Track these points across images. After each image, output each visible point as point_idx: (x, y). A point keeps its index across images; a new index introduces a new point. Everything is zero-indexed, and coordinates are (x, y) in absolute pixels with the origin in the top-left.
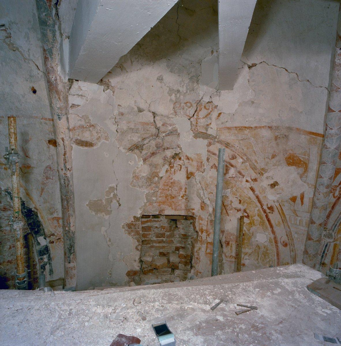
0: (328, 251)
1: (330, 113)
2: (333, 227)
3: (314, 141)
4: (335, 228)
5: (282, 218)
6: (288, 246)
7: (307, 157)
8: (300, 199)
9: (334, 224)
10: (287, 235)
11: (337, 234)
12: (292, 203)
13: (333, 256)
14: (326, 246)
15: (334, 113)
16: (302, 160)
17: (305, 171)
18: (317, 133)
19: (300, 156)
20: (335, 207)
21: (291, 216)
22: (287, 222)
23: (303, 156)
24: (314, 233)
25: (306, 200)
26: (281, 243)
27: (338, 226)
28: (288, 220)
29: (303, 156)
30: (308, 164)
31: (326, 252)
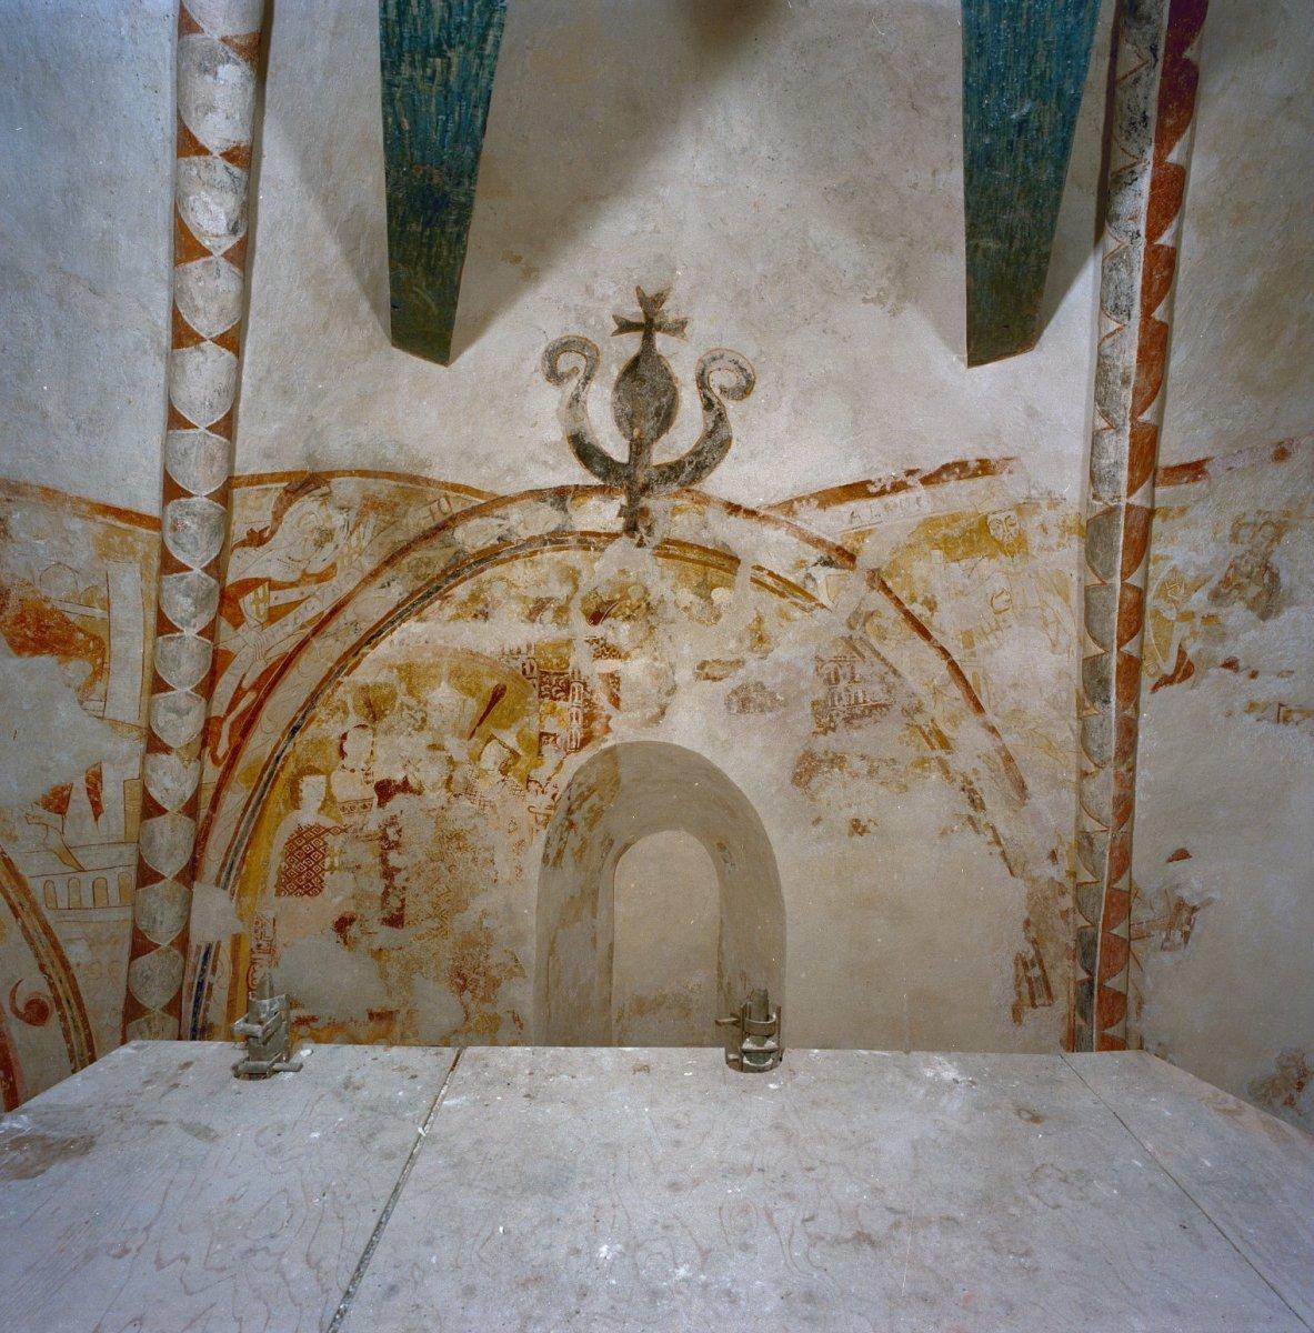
1: (178, 432)
2: (224, 874)
3: (121, 543)
4: (228, 879)
5: (13, 896)
6: (55, 1015)
7: (98, 612)
8: (84, 795)
9: (224, 865)
10: (42, 967)
11: (239, 897)
12: (53, 819)
13: (233, 986)
15: (191, 431)
16: (79, 624)
17: (95, 673)
18: (135, 509)
19: (68, 607)
20: (222, 800)
21: (51, 878)
22: (35, 910)
23: (81, 610)
24: (159, 918)
25: (111, 792)
26: (16, 1012)
28: (39, 899)
29: (81, 610)
30: (107, 643)
31: (209, 978)
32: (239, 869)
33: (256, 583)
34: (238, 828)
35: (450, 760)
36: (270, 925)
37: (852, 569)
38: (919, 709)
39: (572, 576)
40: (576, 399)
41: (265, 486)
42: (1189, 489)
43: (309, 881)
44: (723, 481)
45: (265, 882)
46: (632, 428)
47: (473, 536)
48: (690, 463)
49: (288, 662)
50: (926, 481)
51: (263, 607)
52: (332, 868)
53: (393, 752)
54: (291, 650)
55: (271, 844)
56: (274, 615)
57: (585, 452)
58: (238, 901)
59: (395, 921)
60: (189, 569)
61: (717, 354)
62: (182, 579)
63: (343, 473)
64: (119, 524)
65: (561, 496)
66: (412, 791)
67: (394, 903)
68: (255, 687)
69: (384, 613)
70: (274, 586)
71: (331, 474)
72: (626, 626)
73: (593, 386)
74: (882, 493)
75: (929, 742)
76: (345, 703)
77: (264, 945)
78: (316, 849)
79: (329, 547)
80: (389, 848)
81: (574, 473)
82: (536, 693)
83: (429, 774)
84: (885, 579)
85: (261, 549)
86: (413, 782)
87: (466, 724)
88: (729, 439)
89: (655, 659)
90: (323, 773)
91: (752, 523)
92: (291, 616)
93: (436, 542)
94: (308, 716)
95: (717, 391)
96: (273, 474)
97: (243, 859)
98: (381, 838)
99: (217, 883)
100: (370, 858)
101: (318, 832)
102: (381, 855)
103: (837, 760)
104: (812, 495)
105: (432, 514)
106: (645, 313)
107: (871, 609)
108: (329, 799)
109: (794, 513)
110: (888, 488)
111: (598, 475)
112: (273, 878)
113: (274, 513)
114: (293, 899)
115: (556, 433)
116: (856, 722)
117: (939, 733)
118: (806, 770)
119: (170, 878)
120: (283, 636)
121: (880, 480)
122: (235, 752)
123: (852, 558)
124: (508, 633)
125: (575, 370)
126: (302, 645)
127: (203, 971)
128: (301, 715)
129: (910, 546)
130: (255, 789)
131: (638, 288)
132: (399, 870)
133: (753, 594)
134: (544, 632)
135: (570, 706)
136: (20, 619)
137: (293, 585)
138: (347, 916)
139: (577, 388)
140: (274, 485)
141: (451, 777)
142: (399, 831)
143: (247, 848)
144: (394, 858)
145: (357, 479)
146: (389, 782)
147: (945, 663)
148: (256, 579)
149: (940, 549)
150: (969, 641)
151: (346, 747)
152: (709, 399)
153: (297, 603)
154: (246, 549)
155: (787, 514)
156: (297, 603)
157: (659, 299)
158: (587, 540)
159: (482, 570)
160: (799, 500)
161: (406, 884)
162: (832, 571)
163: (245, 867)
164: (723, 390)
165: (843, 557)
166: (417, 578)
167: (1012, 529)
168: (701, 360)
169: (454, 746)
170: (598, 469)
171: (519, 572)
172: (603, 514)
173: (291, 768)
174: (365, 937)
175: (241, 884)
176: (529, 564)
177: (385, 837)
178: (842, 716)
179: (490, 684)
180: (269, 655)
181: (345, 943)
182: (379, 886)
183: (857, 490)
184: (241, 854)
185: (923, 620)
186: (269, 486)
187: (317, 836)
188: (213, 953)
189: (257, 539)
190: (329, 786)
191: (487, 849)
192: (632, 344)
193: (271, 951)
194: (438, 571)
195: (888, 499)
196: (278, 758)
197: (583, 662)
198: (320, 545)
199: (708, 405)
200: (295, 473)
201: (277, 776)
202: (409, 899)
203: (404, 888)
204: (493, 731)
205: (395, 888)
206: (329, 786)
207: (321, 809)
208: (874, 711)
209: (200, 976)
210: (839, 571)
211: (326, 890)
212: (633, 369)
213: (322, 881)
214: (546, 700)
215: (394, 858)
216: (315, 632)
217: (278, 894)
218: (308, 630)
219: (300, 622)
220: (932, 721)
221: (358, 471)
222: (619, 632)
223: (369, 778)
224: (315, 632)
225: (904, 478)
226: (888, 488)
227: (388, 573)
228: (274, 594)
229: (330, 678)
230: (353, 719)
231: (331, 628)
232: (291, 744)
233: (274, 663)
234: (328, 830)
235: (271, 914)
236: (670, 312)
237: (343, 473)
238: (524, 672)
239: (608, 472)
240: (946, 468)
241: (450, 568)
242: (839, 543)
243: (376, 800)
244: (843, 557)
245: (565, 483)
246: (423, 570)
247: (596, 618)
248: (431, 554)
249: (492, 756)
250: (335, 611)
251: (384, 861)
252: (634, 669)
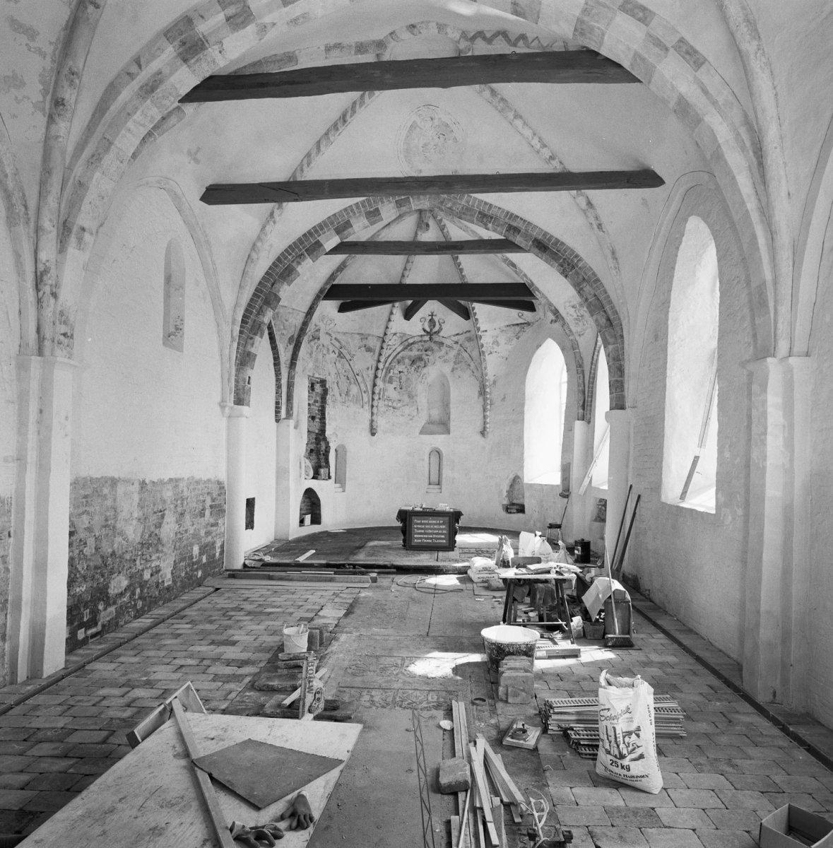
39: (422, 346)
42: (485, 333)
44: (441, 334)
47: (411, 341)
49: (390, 355)
53: (401, 368)
57: (424, 330)
59: (401, 389)
65: (421, 336)
81: (423, 333)
83: (405, 370)
100: (398, 380)
103: (457, 369)
120: (391, 351)
124: (415, 353)
133: (446, 348)
134: (419, 353)
135: (423, 363)
158: (425, 341)
165: (457, 343)
169: (408, 367)
171: (416, 346)
172: (427, 338)
179: (412, 359)
183: (457, 334)
192: (430, 317)
197: (424, 357)
212: (430, 320)
222: (429, 353)
229: (394, 358)
236: (435, 314)
244: (457, 343)
247: (426, 351)
249: (413, 368)
252: (431, 358)
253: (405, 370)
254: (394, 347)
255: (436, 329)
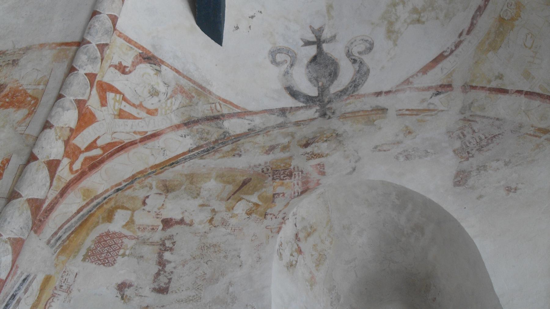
0: (25, 292)
4: (55, 243)
9: (56, 233)
14: (24, 280)
17: (29, 114)
27: (63, 241)
30: (40, 100)
31: (20, 294)
32: (64, 241)
33: (117, 91)
34: (71, 219)
35: (213, 210)
36: (72, 277)
37: (452, 90)
38: (521, 126)
40: (286, 73)
41: (131, 46)
43: (107, 259)
44: (369, 86)
45: (78, 252)
46: (318, 82)
47: (234, 126)
48: (351, 87)
49: (123, 147)
50: (469, 32)
51: (117, 106)
52: (124, 255)
54: (126, 141)
55: (88, 234)
56: (121, 115)
57: (294, 94)
58: (57, 257)
60: (91, 43)
61: (353, 41)
62: (86, 47)
63: (168, 66)
64: (65, 47)
65: (283, 111)
66: (186, 224)
67: (163, 280)
68: (102, 148)
69: (180, 151)
70: (124, 99)
71: (163, 62)
72: (326, 144)
73: (295, 68)
74: (452, 52)
75: (536, 136)
76: (151, 185)
77: (64, 287)
78: (115, 244)
79: (155, 99)
80: (165, 250)
81: (289, 102)
82: (270, 178)
84: (470, 84)
85: (123, 75)
86: (187, 220)
87: (225, 195)
88: (369, 70)
89: (345, 151)
90: (130, 210)
91: (391, 95)
92: (130, 122)
93: (213, 123)
94: (128, 186)
95: (357, 55)
96: (136, 43)
97: (68, 237)
98: (161, 245)
99: (48, 243)
101: (121, 236)
102: (159, 253)
104: (419, 72)
105: (212, 110)
106: (316, 37)
107: (470, 102)
108: (131, 222)
109: (411, 83)
110: (454, 49)
111: (303, 102)
112: (83, 252)
113: (133, 62)
114: (94, 265)
115: (278, 85)
116: (484, 149)
117: (540, 130)
118: (461, 179)
119: (25, 199)
120: (125, 131)
121: (448, 48)
122: (82, 175)
123: (450, 86)
125: (286, 61)
126: (133, 143)
127: (19, 288)
128: (124, 184)
129: (476, 62)
130: (88, 204)
131: (311, 27)
132: (169, 262)
136: (7, 95)
137: (134, 105)
138: (128, 282)
139: (287, 68)
140: (136, 48)
141: (213, 218)
142: (174, 243)
143: (72, 233)
144: (167, 255)
145: (174, 73)
146: (171, 219)
147: (523, 96)
148: (117, 90)
149: (490, 51)
150: (527, 75)
151: (147, 201)
152: (354, 59)
153: (135, 118)
154: (117, 71)
155: (408, 84)
156: (135, 118)
157: (321, 30)
159: (239, 140)
160: (412, 76)
161: (173, 270)
162: (442, 96)
163: (68, 241)
164: (360, 53)
166: (202, 139)
167: (513, 7)
168: (346, 47)
170: (302, 100)
173: (112, 203)
174: (137, 298)
175: (62, 250)
176: (266, 136)
177: (163, 244)
178: (475, 149)
180: (114, 135)
181: (122, 298)
182: (155, 269)
184: (67, 234)
185: (500, 86)
186: (133, 47)
187: (120, 238)
188: (29, 281)
189: (122, 69)
190: (132, 215)
191: (235, 250)
192: (312, 51)
193: (69, 291)
194: (213, 139)
195: (455, 53)
196: (105, 198)
197: (299, 162)
198: (152, 95)
199: (354, 61)
200: (146, 49)
201: (102, 205)
202: (175, 277)
203: (172, 272)
204: (242, 196)
205: (165, 272)
206: (132, 215)
207: (126, 225)
208: (494, 139)
209: (16, 291)
210: (447, 94)
211: (116, 265)
212: (314, 59)
213: (115, 260)
214: (277, 181)
215: (167, 255)
216: (142, 140)
217: (84, 260)
218: (138, 137)
219: (134, 129)
220: (532, 127)
221: (175, 69)
223: (158, 216)
224: (142, 140)
225: (459, 40)
226: (454, 49)
227: (184, 131)
228: (124, 103)
230: (155, 190)
231: (150, 143)
232: (115, 194)
233: (115, 143)
234: (126, 236)
235: (76, 270)
236: (326, 34)
237: (168, 66)
238: (263, 172)
239: (308, 100)
240: (473, 18)
241: (221, 139)
242: (440, 83)
243: (161, 227)
245: (284, 106)
246: (205, 135)
248: (209, 128)
250: (155, 136)
251: (160, 256)
253: (200, 218)
254: (149, 125)
255: (346, 73)
